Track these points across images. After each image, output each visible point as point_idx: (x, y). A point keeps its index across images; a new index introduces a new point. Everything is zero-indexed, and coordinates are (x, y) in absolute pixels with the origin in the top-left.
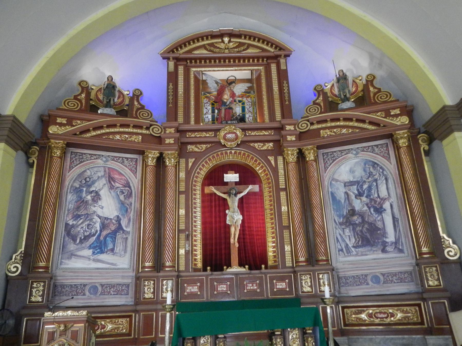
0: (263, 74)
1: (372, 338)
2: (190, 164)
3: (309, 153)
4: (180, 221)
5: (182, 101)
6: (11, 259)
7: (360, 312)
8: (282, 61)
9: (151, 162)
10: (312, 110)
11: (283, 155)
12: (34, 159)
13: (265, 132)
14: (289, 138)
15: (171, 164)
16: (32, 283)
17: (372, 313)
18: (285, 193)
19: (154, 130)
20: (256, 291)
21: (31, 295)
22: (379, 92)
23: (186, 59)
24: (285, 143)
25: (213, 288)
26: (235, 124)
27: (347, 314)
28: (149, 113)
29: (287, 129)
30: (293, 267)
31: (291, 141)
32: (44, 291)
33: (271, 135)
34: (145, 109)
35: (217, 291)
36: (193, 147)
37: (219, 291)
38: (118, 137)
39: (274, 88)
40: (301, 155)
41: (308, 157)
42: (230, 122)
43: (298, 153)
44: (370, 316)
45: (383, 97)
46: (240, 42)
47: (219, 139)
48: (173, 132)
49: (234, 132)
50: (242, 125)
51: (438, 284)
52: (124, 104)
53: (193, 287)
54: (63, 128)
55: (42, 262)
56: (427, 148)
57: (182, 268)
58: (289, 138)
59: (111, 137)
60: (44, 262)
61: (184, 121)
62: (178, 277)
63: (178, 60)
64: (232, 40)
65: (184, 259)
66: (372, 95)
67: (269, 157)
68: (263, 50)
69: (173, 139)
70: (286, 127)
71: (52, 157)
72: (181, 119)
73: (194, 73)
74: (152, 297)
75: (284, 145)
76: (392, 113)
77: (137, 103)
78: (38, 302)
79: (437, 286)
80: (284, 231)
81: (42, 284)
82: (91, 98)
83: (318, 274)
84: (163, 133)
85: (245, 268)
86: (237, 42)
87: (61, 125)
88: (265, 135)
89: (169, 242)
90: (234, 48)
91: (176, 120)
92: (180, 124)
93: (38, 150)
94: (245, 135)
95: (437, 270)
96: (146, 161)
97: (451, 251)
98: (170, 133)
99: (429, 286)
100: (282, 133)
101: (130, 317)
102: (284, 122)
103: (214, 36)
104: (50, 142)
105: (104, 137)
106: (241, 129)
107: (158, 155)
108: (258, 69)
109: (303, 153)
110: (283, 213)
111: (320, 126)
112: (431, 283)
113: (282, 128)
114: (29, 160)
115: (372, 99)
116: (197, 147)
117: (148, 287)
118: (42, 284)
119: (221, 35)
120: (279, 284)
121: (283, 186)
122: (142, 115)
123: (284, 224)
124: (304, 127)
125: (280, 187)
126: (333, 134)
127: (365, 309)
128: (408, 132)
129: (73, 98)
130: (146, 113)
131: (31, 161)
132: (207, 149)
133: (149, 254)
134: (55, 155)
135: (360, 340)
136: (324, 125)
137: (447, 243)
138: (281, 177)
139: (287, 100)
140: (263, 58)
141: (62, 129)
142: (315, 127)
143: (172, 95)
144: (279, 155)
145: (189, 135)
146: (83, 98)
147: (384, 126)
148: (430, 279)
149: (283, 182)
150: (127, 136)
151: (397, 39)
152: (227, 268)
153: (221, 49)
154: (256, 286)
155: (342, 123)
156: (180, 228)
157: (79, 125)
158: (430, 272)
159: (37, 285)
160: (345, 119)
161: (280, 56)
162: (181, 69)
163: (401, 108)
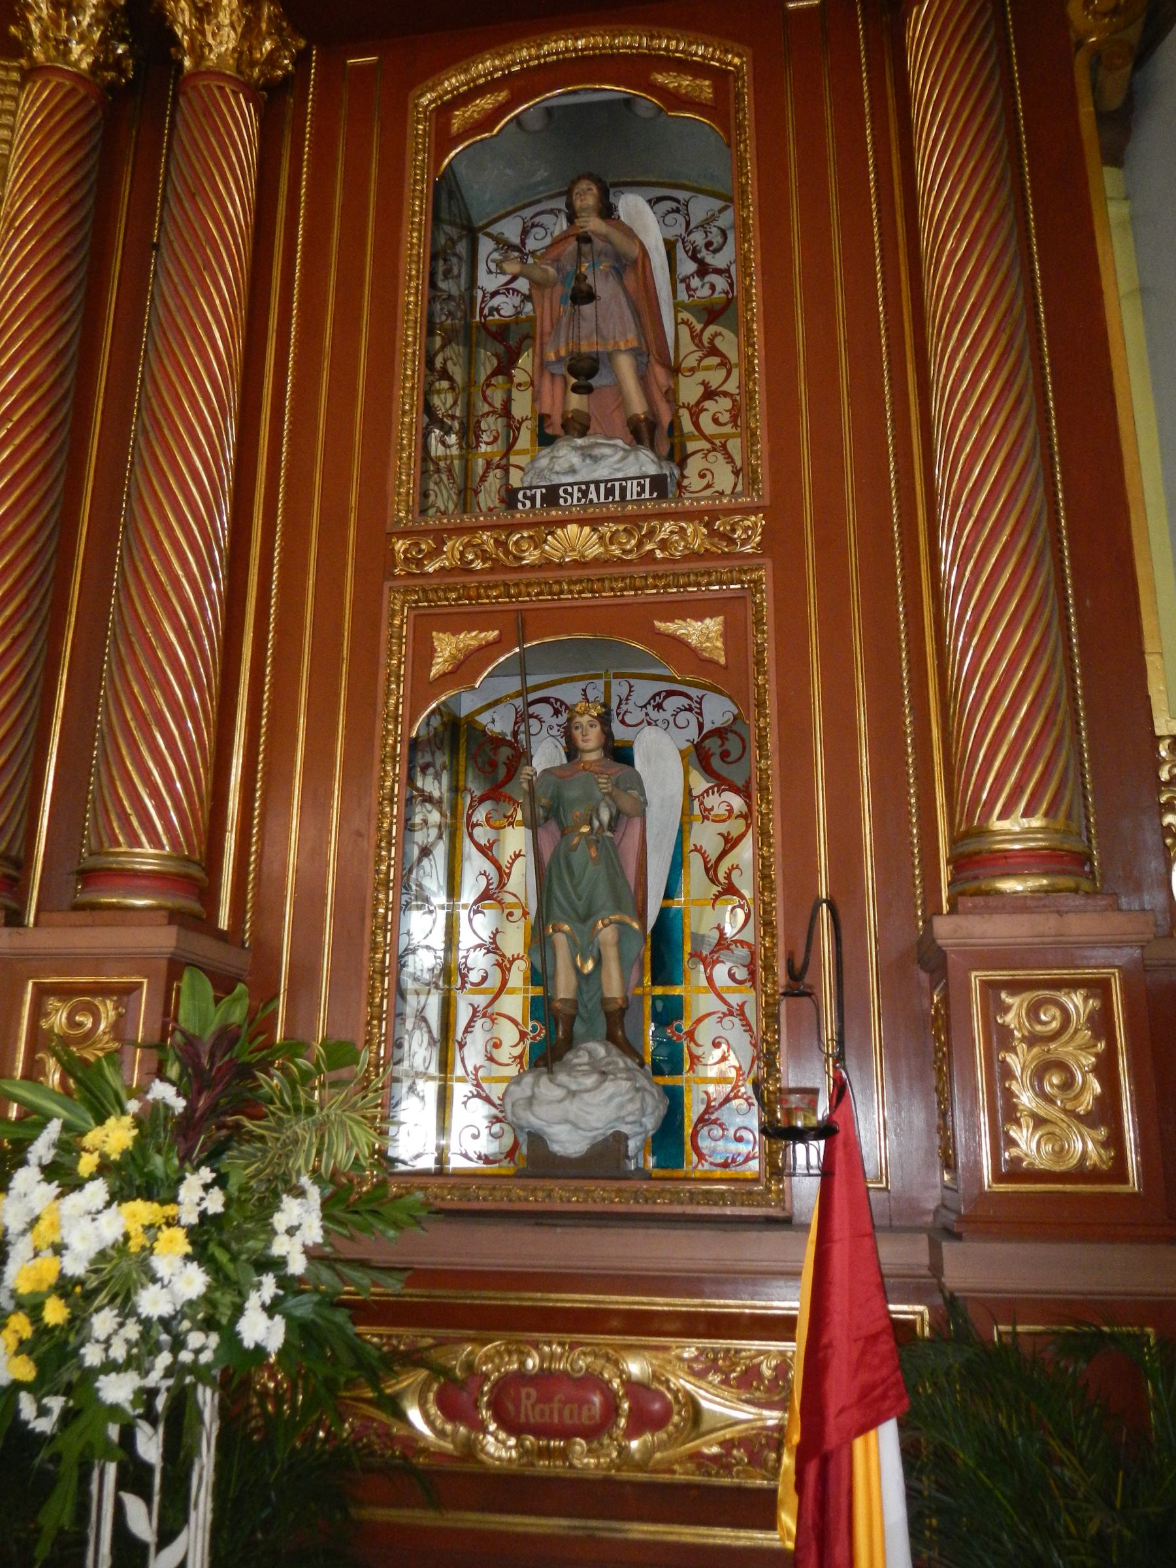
83: (42, 992)
148: (1026, 1099)
158: (1033, 1040)
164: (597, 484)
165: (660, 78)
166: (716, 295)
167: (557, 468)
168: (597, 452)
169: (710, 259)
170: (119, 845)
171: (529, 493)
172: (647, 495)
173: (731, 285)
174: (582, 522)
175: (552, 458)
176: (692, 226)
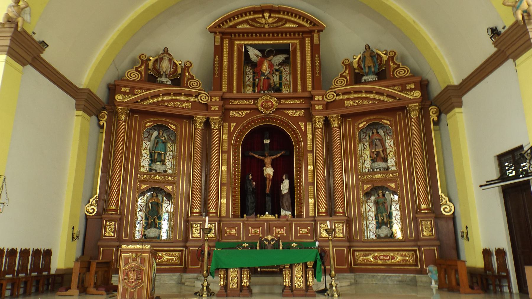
0: (298, 47)
1: (374, 275)
2: (232, 128)
3: (334, 121)
4: (223, 176)
5: (226, 71)
6: (89, 202)
7: (368, 255)
8: (316, 36)
9: (199, 127)
11: (312, 122)
12: (103, 122)
13: (297, 101)
15: (216, 128)
16: (106, 223)
17: (377, 256)
19: (202, 98)
20: (283, 235)
21: (105, 231)
23: (230, 34)
24: (313, 112)
25: (248, 231)
26: (270, 94)
27: (357, 255)
28: (199, 84)
29: (316, 99)
30: (315, 217)
31: (319, 110)
32: (115, 228)
33: (302, 104)
34: (195, 79)
35: (251, 233)
36: (235, 113)
37: (253, 234)
38: (171, 104)
39: (307, 61)
40: (327, 122)
41: (333, 123)
42: (266, 92)
43: (324, 121)
44: (375, 258)
45: (401, 73)
46: (279, 18)
47: (257, 107)
48: (218, 100)
49: (270, 101)
50: (278, 95)
51: (431, 234)
52: (177, 74)
53: (232, 230)
54: (127, 97)
55: (113, 206)
56: (436, 119)
57: (224, 214)
59: (166, 104)
60: (115, 206)
61: (227, 90)
62: (220, 221)
63: (223, 34)
64: (272, 15)
65: (225, 207)
68: (300, 25)
69: (218, 106)
71: (118, 121)
72: (225, 88)
73: (237, 46)
74: (199, 236)
75: (313, 113)
76: (408, 88)
77: (188, 74)
78: (111, 236)
79: (430, 236)
80: (309, 187)
81: (114, 223)
82: (149, 68)
83: (334, 223)
84: (209, 101)
85: (275, 216)
86: (276, 17)
87: (125, 93)
88: (297, 104)
89: (213, 193)
90: (273, 23)
91: (221, 89)
92: (224, 93)
93: (106, 114)
94: (280, 103)
95: (431, 223)
96: (195, 125)
97: (447, 208)
98: (215, 101)
99: (423, 236)
100: (311, 103)
101: (181, 251)
103: (255, 11)
104: (117, 109)
105: (160, 104)
106: (276, 98)
107: (205, 120)
108: (294, 43)
109: (329, 121)
111: (344, 97)
112: (425, 233)
113: (311, 98)
114: (100, 122)
116: (239, 113)
117: (196, 229)
118: (114, 223)
119: (261, 11)
120: (302, 230)
122: (192, 84)
123: (309, 181)
124: (331, 97)
125: (308, 149)
126: (356, 104)
127: (372, 252)
128: (419, 105)
129: (134, 70)
130: (195, 83)
131: (102, 124)
132: (246, 114)
133: (197, 202)
134: (120, 119)
135: (365, 276)
136: (348, 96)
137: (444, 201)
139: (317, 73)
140: (299, 33)
141: (126, 97)
142: (341, 97)
143: (218, 67)
144: (308, 122)
145: (231, 103)
146: (142, 70)
147: (399, 99)
148: (425, 230)
150: (179, 103)
151: (414, 22)
152: (260, 216)
153: (262, 24)
154: (283, 231)
155: (364, 95)
156: (223, 182)
157: (140, 93)
159: (109, 223)
160: (367, 92)
161: (314, 31)
162: (226, 43)
163: (415, 83)
165: (383, 121)
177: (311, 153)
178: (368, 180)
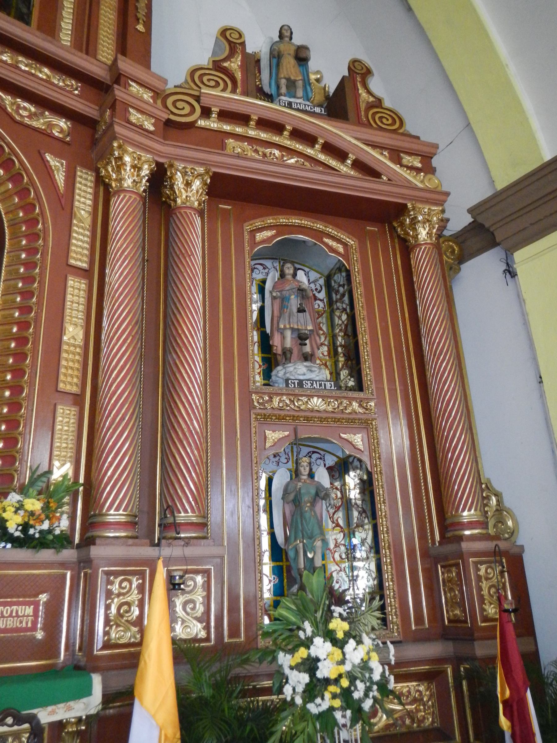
3: (188, 184)
10: (209, 80)
14: (135, 116)
18: (83, 285)
22: (377, 107)
31: (141, 127)
33: (70, 92)
58: (135, 116)
66: (363, 106)
67: (48, 157)
70: (130, 85)
100: (117, 92)
102: (125, 65)
110: (65, 347)
111: (227, 128)
115: (363, 113)
121: (80, 260)
123: (61, 386)
125: (72, 262)
136: (239, 130)
138: (77, 233)
139: (141, 21)
142: (213, 124)
149: (83, 248)
164: (316, 381)
166: (320, 308)
167: (298, 372)
168: (313, 369)
169: (317, 294)
170: (180, 513)
171: (293, 381)
172: (333, 388)
173: (325, 306)
174: (319, 397)
175: (295, 368)
176: (311, 281)
177: (84, 277)
178: (282, 413)
